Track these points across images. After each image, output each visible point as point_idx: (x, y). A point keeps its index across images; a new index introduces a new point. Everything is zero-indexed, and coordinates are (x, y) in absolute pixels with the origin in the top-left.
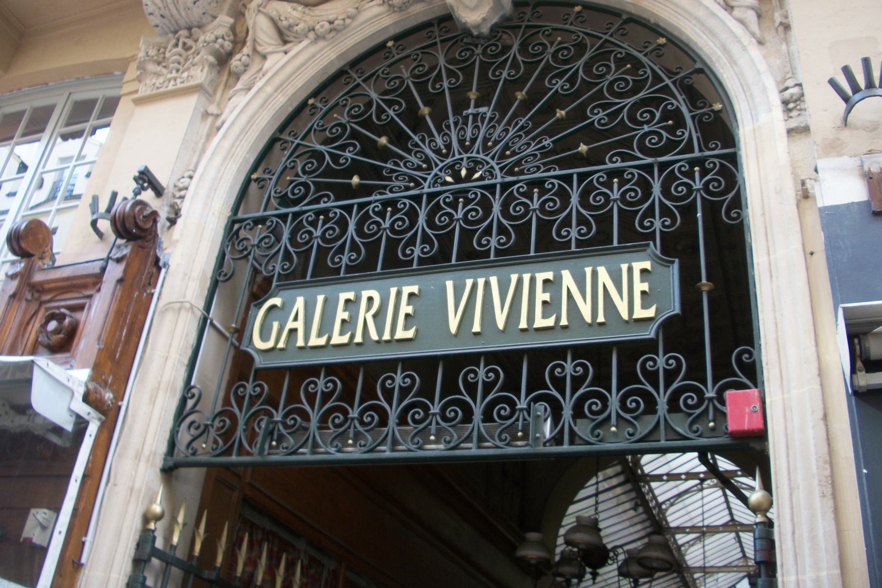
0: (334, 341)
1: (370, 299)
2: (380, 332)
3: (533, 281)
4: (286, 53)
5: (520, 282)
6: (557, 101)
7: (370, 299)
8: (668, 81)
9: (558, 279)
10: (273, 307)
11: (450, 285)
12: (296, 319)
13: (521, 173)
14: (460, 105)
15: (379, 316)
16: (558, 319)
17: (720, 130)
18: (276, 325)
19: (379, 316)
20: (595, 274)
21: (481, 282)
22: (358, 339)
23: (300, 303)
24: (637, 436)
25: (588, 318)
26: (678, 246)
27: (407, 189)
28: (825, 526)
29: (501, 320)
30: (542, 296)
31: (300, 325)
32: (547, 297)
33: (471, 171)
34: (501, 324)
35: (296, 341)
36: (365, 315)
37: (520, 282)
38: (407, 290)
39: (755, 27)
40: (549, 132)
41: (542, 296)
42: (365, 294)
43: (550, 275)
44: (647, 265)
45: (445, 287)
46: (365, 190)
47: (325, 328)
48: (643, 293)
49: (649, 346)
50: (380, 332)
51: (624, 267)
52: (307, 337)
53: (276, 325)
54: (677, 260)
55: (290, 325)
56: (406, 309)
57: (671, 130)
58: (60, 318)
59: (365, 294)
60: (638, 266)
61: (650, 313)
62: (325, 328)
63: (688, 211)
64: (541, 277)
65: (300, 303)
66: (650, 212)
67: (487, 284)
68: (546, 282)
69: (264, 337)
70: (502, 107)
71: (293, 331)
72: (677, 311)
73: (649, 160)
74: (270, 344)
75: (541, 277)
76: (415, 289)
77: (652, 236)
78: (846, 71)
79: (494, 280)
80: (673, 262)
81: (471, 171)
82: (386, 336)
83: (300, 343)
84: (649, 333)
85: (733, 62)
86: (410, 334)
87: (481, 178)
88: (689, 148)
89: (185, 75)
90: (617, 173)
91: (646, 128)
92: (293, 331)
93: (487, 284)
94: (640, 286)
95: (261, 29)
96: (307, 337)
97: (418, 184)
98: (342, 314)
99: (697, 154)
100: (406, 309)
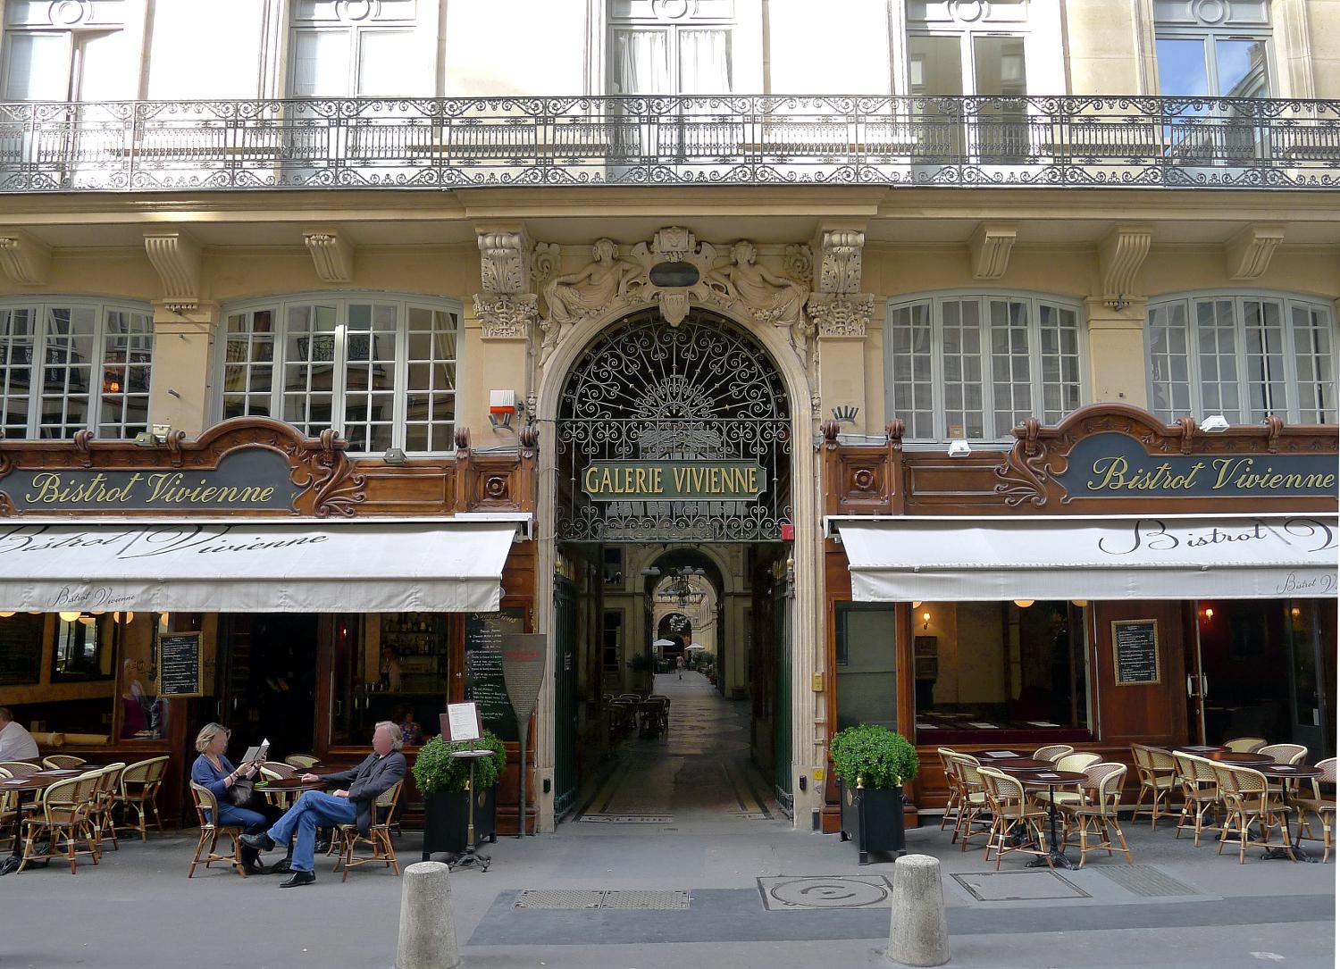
1: (640, 473)
4: (574, 324)
6: (716, 379)
7: (640, 473)
8: (764, 377)
9: (720, 471)
13: (700, 416)
14: (669, 372)
17: (784, 407)
21: (689, 469)
22: (638, 491)
26: (765, 460)
27: (648, 416)
28: (811, 575)
31: (609, 482)
33: (678, 411)
38: (657, 470)
39: (804, 361)
40: (713, 395)
43: (717, 470)
44: (755, 470)
46: (627, 414)
49: (755, 503)
52: (614, 489)
55: (604, 482)
57: (765, 404)
58: (498, 482)
59: (638, 470)
60: (751, 470)
63: (770, 446)
66: (755, 444)
70: (690, 377)
71: (606, 485)
73: (755, 418)
75: (713, 470)
77: (755, 456)
78: (839, 409)
81: (678, 411)
85: (793, 379)
87: (683, 416)
88: (771, 416)
89: (513, 328)
90: (743, 423)
91: (754, 402)
92: (606, 485)
95: (556, 306)
96: (614, 489)
97: (653, 415)
98: (628, 479)
99: (775, 419)
100: (657, 480)
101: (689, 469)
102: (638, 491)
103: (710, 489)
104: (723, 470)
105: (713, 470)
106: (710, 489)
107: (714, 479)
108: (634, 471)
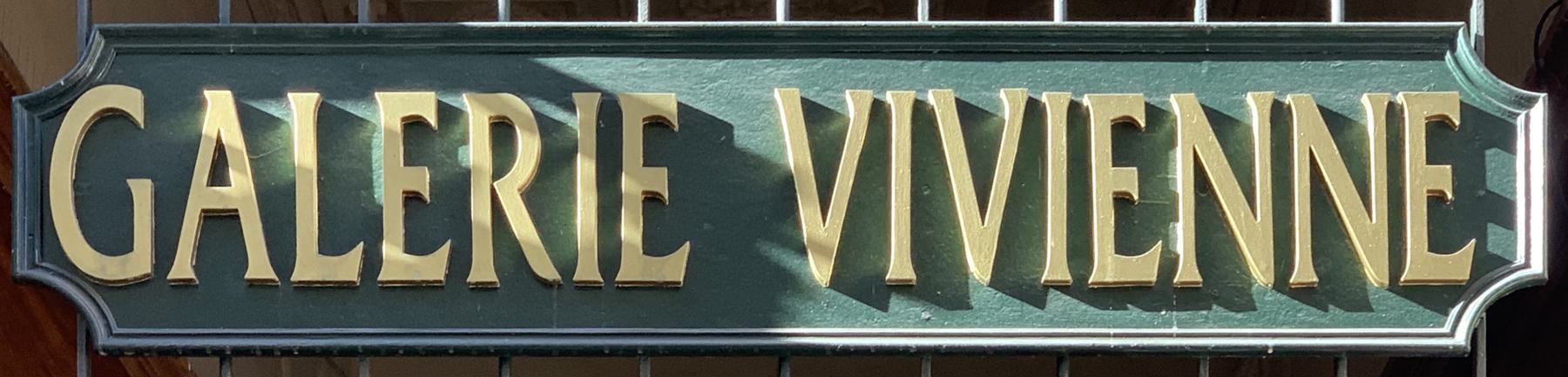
3: (1077, 117)
5: (1034, 112)
7: (502, 131)
10: (111, 117)
12: (218, 175)
18: (142, 191)
20: (1280, 116)
22: (483, 269)
23: (219, 114)
30: (1110, 179)
35: (244, 264)
37: (1034, 112)
52: (282, 248)
53: (142, 191)
54: (1542, 96)
55: (201, 197)
61: (1457, 265)
64: (1102, 111)
65: (219, 114)
67: (923, 117)
68: (1123, 129)
69: (110, 235)
72: (1538, 266)
74: (139, 262)
80: (1528, 103)
83: (259, 266)
86: (673, 267)
92: (222, 223)
93: (923, 117)
94: (1426, 179)
96: (282, 248)
102: (483, 269)
103: (1079, 250)
104: (1183, 107)
105: (1102, 111)
106: (1079, 250)
107: (1110, 179)
108: (448, 114)
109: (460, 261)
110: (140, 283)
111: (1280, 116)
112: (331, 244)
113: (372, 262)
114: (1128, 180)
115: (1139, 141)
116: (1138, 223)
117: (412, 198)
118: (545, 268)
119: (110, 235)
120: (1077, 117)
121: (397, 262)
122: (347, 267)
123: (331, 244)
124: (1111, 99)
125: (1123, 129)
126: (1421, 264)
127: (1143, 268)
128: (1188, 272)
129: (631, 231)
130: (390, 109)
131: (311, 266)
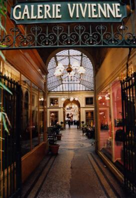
0: (38, 18)
1: (47, 7)
2: (52, 15)
3: (91, 6)
5: (88, 6)
7: (47, 7)
9: (97, 6)
10: (18, 8)
11: (69, 5)
12: (26, 11)
15: (51, 12)
16: (98, 16)
19: (51, 12)
20: (106, 6)
21: (77, 5)
22: (46, 17)
23: (26, 7)
24: (119, 43)
25: (106, 16)
29: (84, 15)
30: (94, 10)
31: (27, 13)
32: (95, 10)
34: (84, 16)
36: (46, 12)
37: (88, 6)
41: (94, 10)
42: (46, 6)
43: (95, 5)
45: (68, 6)
47: (36, 14)
48: (118, 12)
50: (52, 15)
51: (113, 4)
55: (24, 13)
56: (58, 10)
59: (46, 6)
61: (120, 16)
62: (36, 14)
65: (26, 7)
67: (79, 6)
71: (26, 15)
74: (19, 18)
76: (60, 5)
79: (81, 5)
82: (54, 17)
83: (28, 17)
84: (120, 21)
86: (60, 17)
92: (26, 15)
93: (79, 6)
98: (39, 11)
100: (58, 10)
101: (77, 5)
103: (91, 15)
104: (99, 5)
106: (91, 15)
108: (44, 6)
109: (44, 17)
110: (20, 19)
111: (106, 6)
112: (34, 16)
113: (37, 17)
114: (95, 10)
115: (96, 7)
116: (96, 13)
117: (40, 13)
118: (50, 17)
119: (17, 15)
120: (91, 6)
121: (39, 17)
122: (35, 17)
123: (34, 16)
124: (93, 5)
125: (94, 6)
126: (118, 16)
127: (96, 16)
128: (100, 16)
129: (57, 13)
130: (39, 6)
131: (33, 17)
